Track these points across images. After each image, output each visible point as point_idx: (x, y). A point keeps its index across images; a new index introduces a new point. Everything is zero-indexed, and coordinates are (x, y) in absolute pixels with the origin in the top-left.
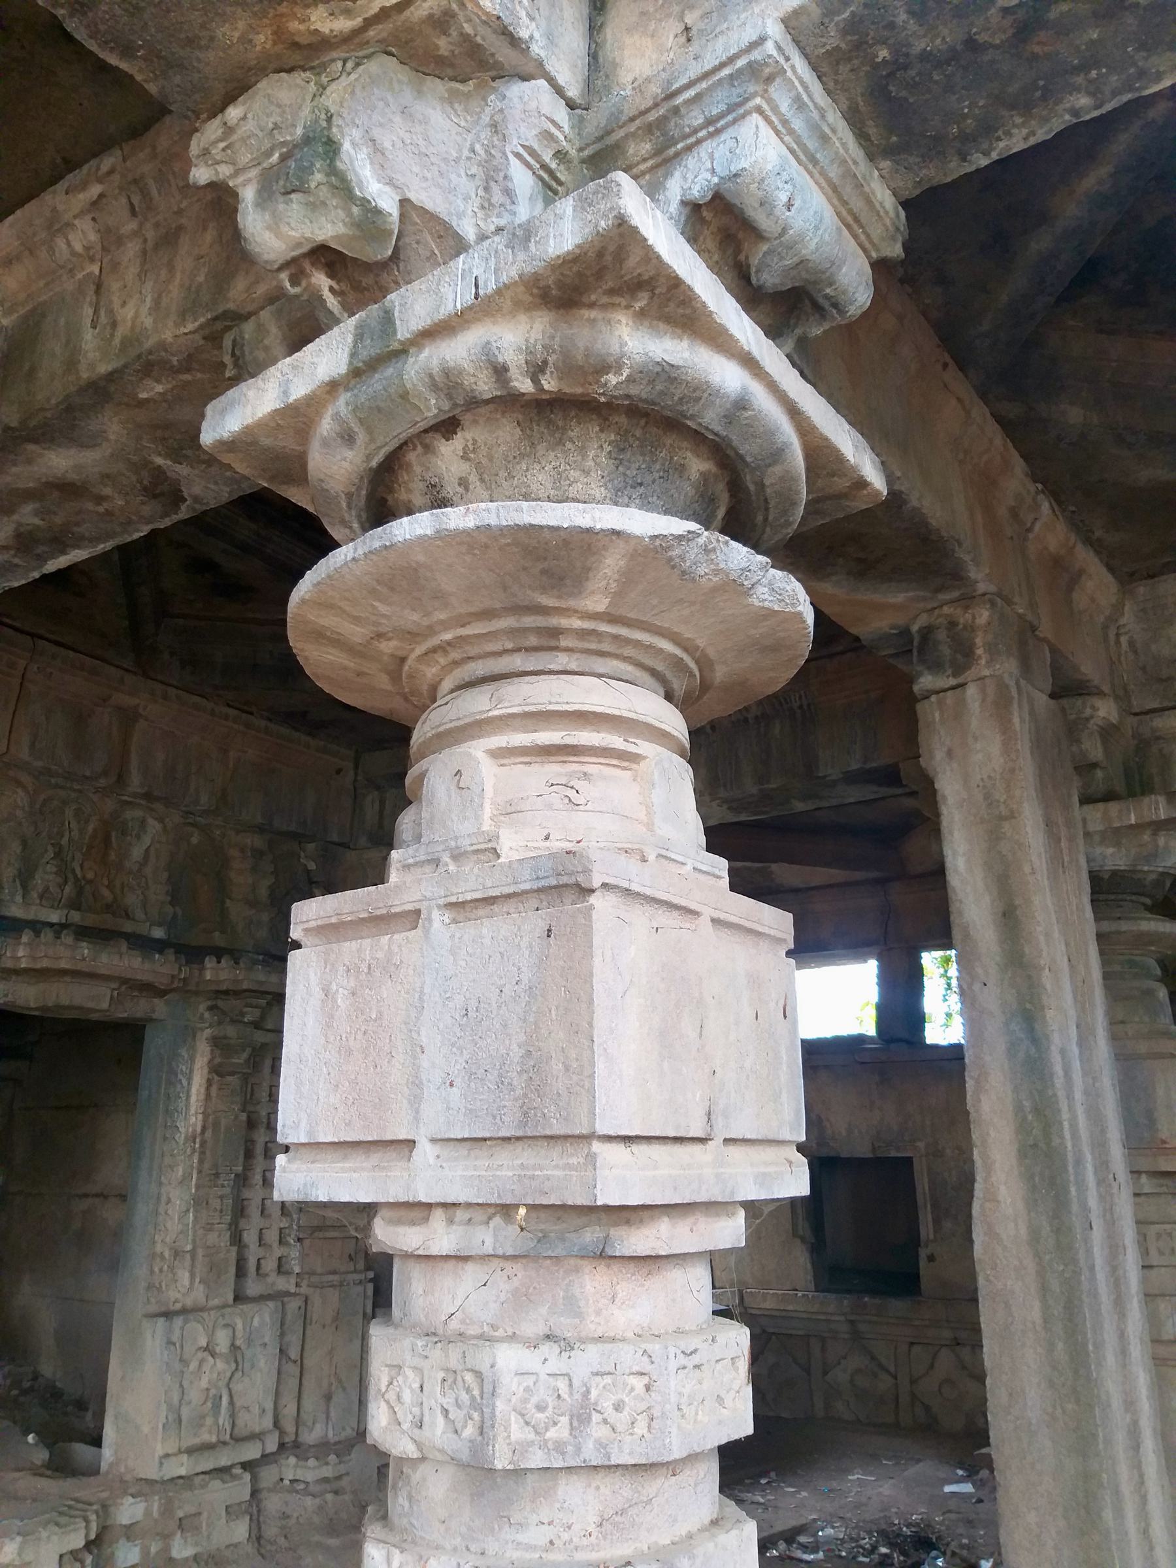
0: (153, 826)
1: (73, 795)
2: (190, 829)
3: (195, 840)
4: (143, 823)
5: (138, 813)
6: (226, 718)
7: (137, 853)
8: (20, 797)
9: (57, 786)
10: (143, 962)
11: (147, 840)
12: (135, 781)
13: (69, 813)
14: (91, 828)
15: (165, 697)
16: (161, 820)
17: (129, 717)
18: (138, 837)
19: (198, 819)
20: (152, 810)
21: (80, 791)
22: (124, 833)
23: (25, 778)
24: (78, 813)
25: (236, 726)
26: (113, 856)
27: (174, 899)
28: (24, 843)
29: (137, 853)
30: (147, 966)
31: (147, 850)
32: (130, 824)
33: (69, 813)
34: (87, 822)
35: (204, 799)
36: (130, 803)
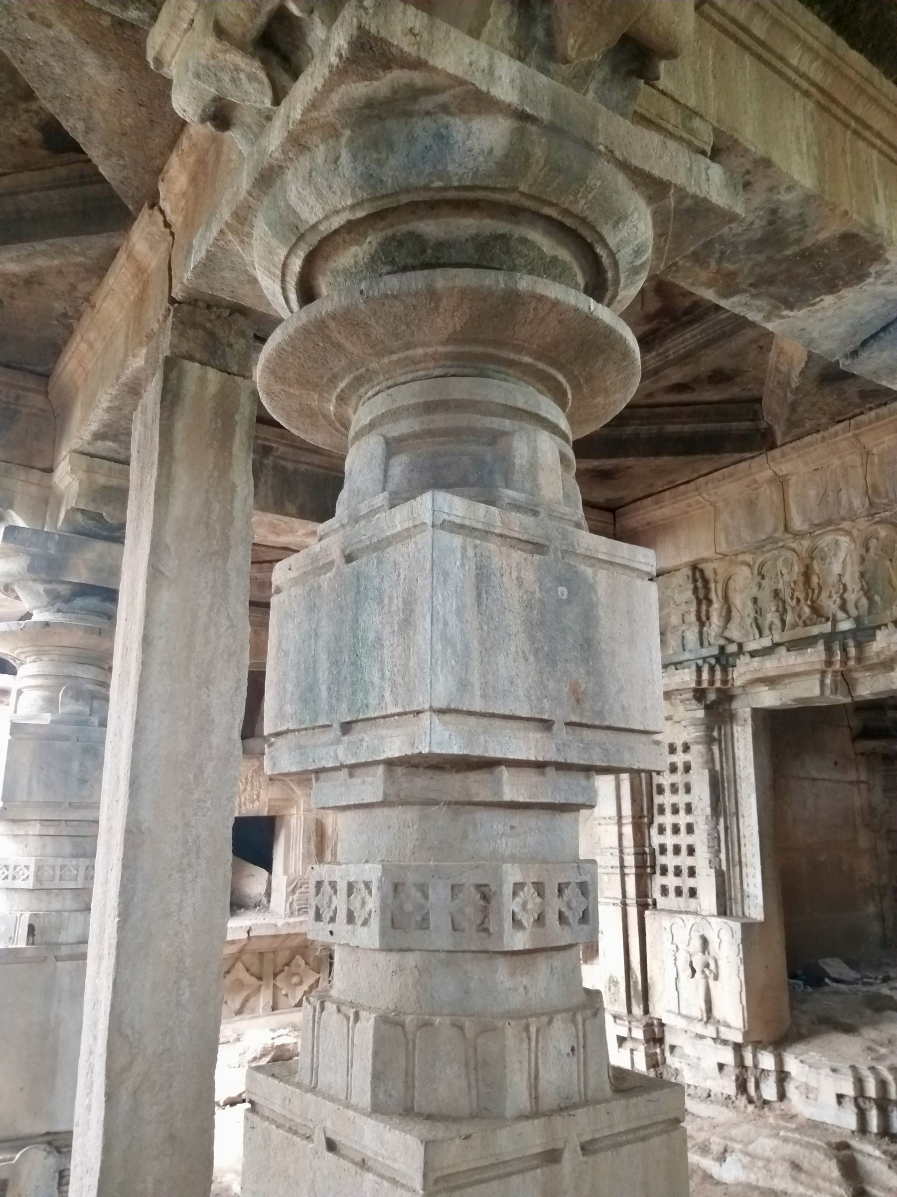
0: (844, 540)
1: (776, 552)
2: (874, 527)
3: (883, 533)
4: (837, 543)
5: (829, 538)
6: (836, 434)
7: (836, 568)
8: (746, 570)
9: (769, 551)
10: (796, 659)
11: (842, 554)
12: (798, 523)
13: (780, 564)
14: (796, 568)
15: (783, 455)
16: (848, 533)
17: (781, 482)
18: (835, 555)
19: (883, 514)
20: (839, 530)
21: (782, 547)
22: (823, 559)
23: (748, 558)
24: (786, 560)
25: (850, 434)
26: (815, 580)
27: (867, 593)
28: (755, 600)
29: (836, 568)
30: (800, 660)
31: (844, 562)
32: (826, 549)
33: (780, 564)
34: (792, 565)
35: (857, 503)
36: (823, 533)
